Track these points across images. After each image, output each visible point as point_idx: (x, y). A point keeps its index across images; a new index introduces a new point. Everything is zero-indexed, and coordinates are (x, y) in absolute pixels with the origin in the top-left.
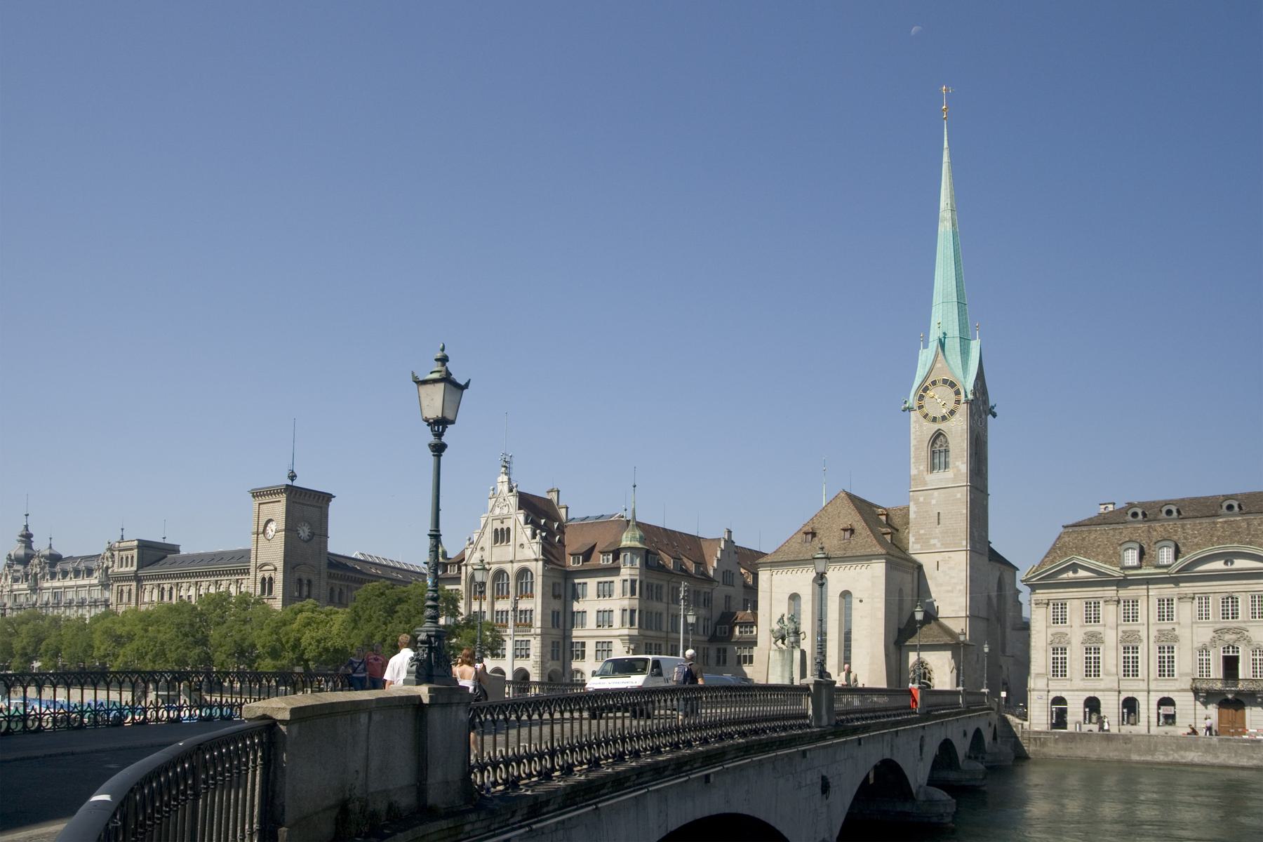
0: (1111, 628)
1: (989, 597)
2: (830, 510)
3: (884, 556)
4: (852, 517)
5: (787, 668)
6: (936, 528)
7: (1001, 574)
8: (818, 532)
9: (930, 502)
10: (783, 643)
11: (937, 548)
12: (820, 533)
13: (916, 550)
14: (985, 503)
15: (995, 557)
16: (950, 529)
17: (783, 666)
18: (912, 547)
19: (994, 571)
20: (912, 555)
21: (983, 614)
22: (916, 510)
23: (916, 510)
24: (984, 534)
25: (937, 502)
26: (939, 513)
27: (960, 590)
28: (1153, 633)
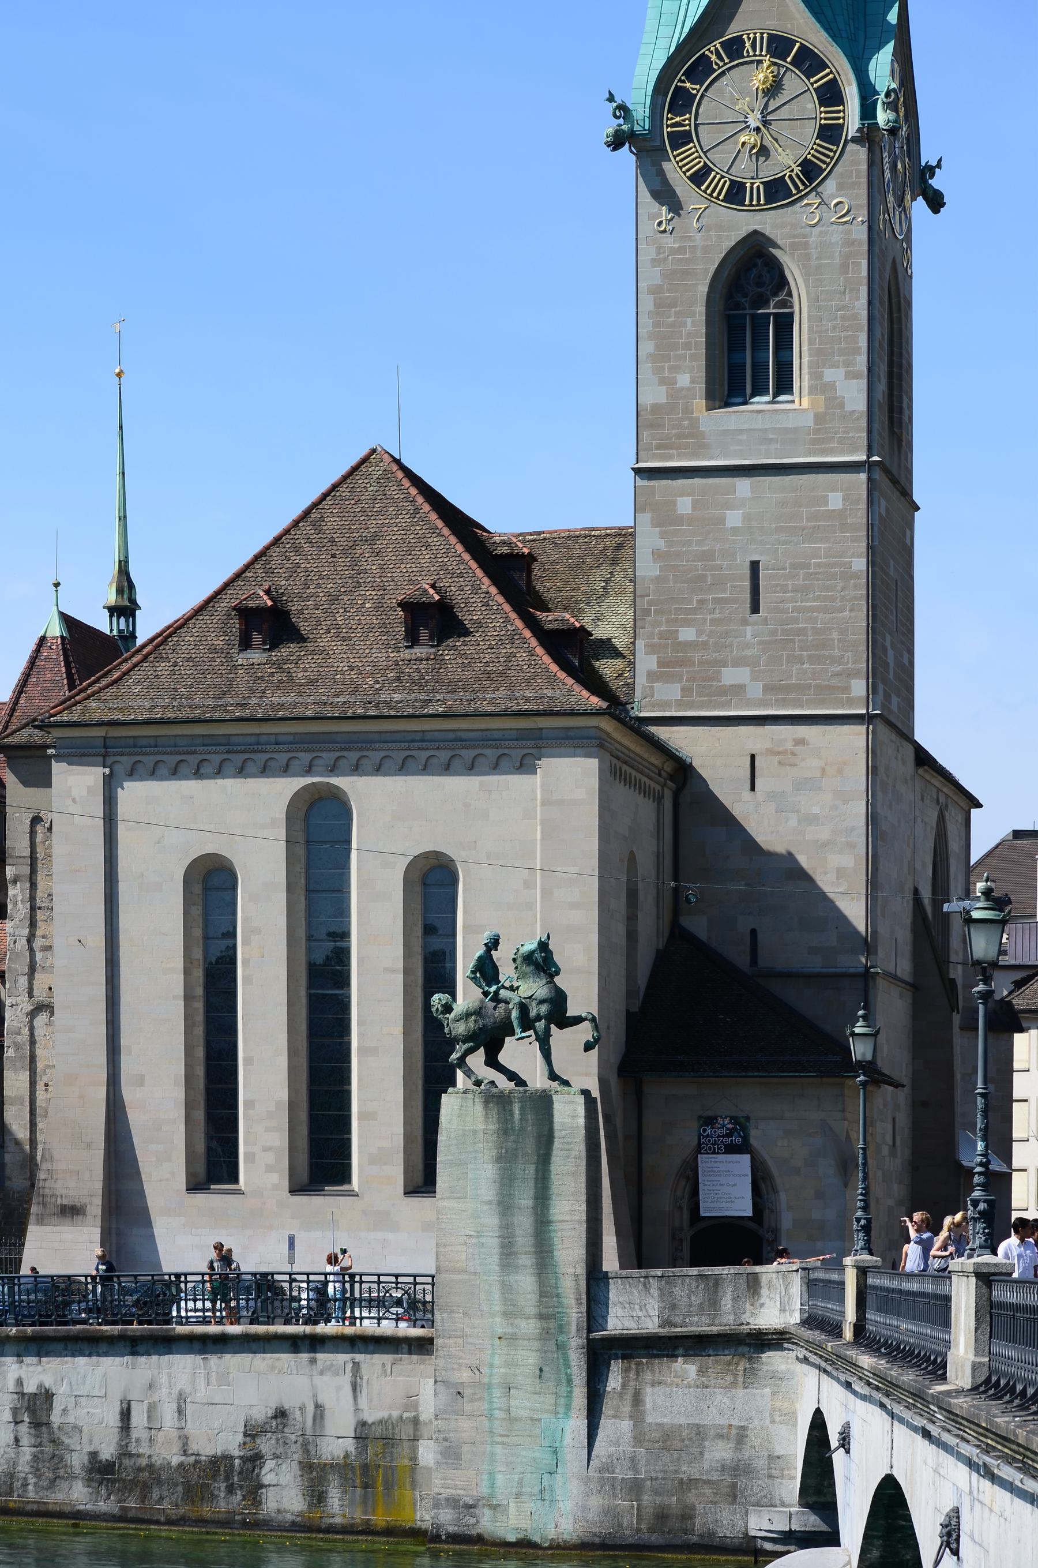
2: (332, 523)
3: (593, 722)
5: (528, 1170)
6: (745, 622)
7: (941, 820)
8: (293, 607)
9: (722, 520)
10: (492, 1061)
11: (749, 704)
13: (665, 705)
14: (908, 542)
16: (801, 632)
17: (505, 1159)
18: (649, 693)
20: (653, 729)
22: (661, 544)
23: (661, 544)
24: (906, 655)
25: (747, 518)
26: (755, 566)
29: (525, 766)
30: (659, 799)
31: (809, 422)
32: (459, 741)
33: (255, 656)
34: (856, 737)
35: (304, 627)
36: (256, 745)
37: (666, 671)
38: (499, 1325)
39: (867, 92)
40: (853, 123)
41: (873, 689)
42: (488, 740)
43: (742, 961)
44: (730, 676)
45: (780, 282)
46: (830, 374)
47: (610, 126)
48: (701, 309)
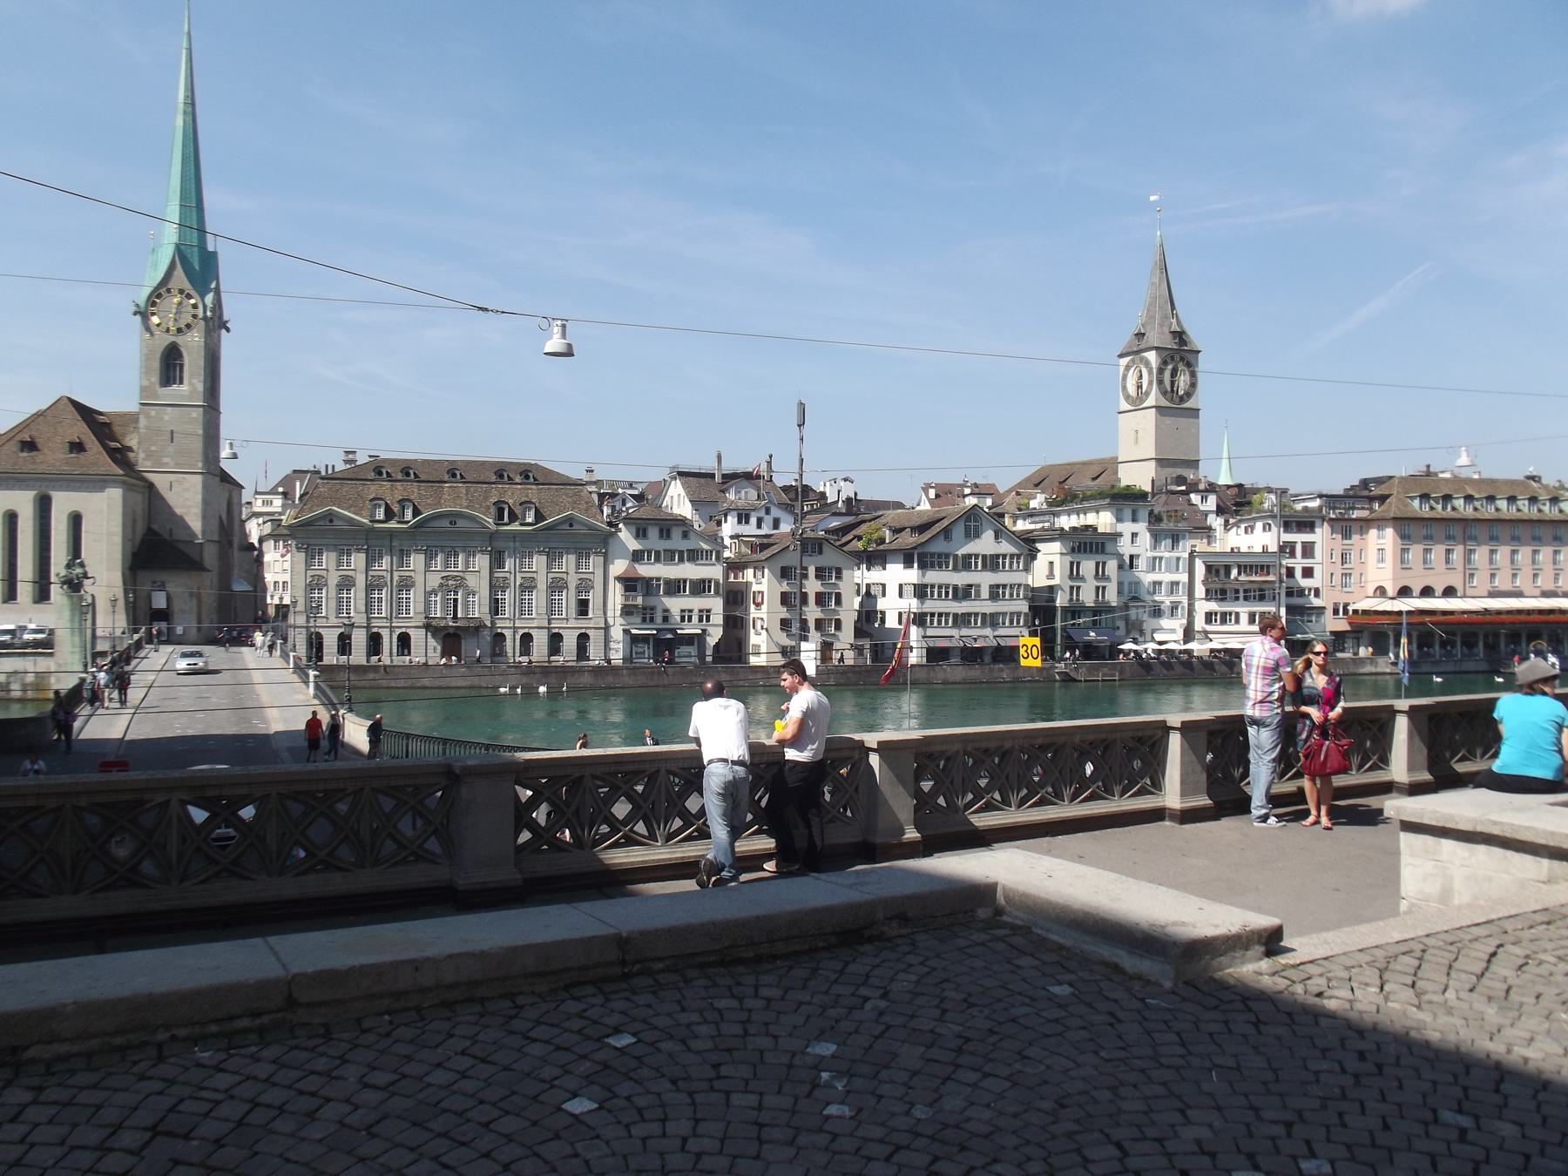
0: (361, 572)
1: (220, 518)
4: (80, 431)
8: (37, 440)
12: (40, 442)
15: (225, 478)
19: (223, 492)
21: (216, 538)
26: (172, 432)
27: (195, 514)
28: (396, 578)
29: (102, 489)
30: (144, 493)
31: (187, 393)
32: (83, 481)
33: (25, 454)
34: (199, 478)
35: (40, 446)
36: (24, 480)
37: (147, 457)
38: (71, 649)
39: (205, 307)
40: (201, 315)
41: (204, 465)
42: (93, 481)
43: (168, 537)
44: (166, 460)
45: (181, 356)
46: (194, 381)
47: (134, 309)
48: (158, 360)
